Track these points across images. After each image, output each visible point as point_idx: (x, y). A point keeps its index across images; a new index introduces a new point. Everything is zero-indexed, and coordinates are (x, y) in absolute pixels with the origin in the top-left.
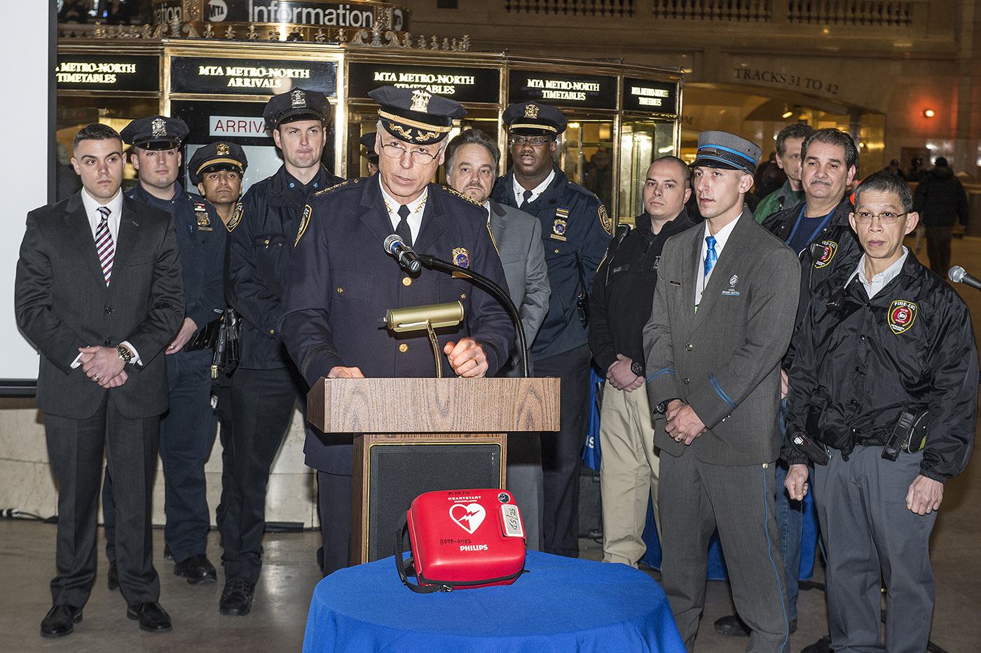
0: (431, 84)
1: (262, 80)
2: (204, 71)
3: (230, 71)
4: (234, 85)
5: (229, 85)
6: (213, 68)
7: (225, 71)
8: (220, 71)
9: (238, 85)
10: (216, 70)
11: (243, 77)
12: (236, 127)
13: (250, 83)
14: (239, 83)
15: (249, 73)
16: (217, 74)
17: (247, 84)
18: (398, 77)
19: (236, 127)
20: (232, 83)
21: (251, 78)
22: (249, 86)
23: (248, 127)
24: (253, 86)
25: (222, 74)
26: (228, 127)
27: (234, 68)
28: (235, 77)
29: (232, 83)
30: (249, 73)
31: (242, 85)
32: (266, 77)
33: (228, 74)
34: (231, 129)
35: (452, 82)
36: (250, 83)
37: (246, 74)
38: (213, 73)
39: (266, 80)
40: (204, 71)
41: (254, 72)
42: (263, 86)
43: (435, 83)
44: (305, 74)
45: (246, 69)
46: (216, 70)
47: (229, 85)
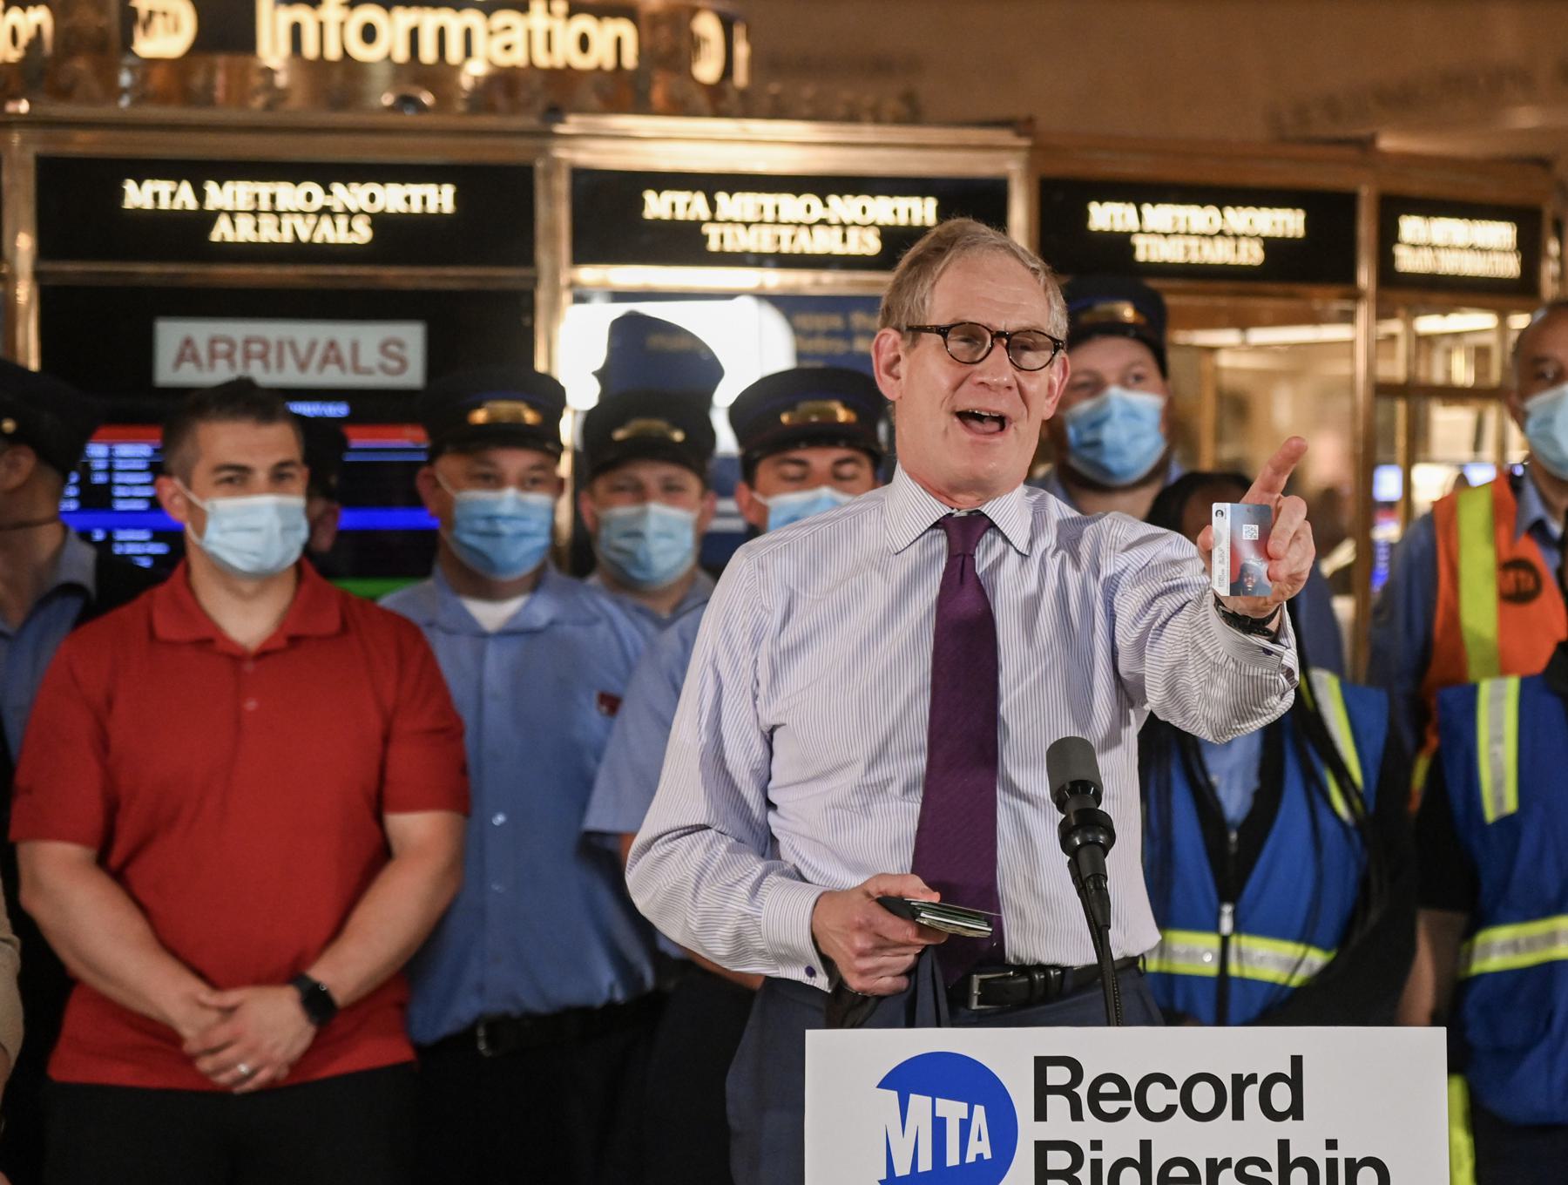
0: (810, 226)
1: (312, 220)
2: (138, 196)
3: (219, 195)
4: (230, 238)
5: (215, 237)
6: (164, 187)
7: (200, 195)
8: (185, 198)
9: (241, 239)
10: (173, 195)
11: (255, 213)
12: (238, 356)
13: (279, 229)
14: (244, 232)
15: (273, 198)
16: (177, 206)
17: (269, 233)
18: (713, 206)
19: (238, 356)
20: (222, 231)
21: (278, 214)
22: (275, 237)
23: (272, 357)
24: (287, 237)
25: (192, 204)
26: (213, 355)
27: (229, 185)
28: (232, 214)
29: (222, 231)
30: (273, 198)
31: (253, 238)
32: (320, 213)
33: (210, 205)
34: (221, 364)
35: (868, 219)
36: (279, 229)
37: (265, 204)
38: (164, 204)
39: (326, 221)
40: (138, 196)
41: (289, 195)
42: (318, 239)
43: (823, 222)
44: (440, 198)
45: (264, 189)
46: (173, 195)
47: (215, 237)
